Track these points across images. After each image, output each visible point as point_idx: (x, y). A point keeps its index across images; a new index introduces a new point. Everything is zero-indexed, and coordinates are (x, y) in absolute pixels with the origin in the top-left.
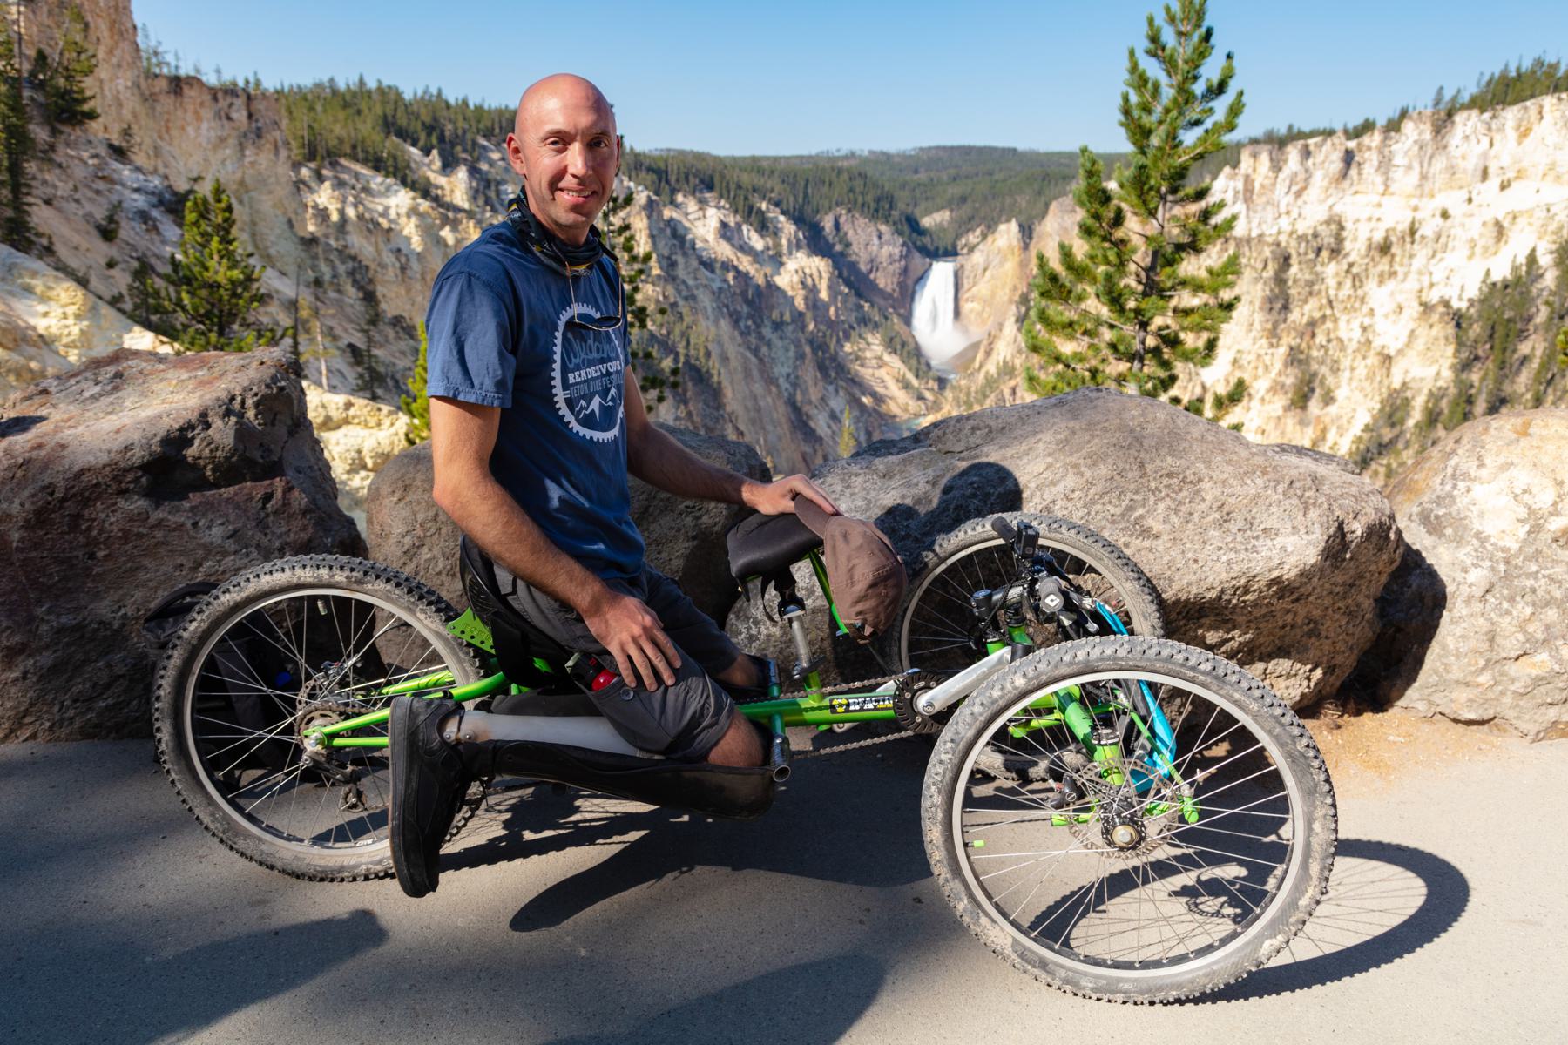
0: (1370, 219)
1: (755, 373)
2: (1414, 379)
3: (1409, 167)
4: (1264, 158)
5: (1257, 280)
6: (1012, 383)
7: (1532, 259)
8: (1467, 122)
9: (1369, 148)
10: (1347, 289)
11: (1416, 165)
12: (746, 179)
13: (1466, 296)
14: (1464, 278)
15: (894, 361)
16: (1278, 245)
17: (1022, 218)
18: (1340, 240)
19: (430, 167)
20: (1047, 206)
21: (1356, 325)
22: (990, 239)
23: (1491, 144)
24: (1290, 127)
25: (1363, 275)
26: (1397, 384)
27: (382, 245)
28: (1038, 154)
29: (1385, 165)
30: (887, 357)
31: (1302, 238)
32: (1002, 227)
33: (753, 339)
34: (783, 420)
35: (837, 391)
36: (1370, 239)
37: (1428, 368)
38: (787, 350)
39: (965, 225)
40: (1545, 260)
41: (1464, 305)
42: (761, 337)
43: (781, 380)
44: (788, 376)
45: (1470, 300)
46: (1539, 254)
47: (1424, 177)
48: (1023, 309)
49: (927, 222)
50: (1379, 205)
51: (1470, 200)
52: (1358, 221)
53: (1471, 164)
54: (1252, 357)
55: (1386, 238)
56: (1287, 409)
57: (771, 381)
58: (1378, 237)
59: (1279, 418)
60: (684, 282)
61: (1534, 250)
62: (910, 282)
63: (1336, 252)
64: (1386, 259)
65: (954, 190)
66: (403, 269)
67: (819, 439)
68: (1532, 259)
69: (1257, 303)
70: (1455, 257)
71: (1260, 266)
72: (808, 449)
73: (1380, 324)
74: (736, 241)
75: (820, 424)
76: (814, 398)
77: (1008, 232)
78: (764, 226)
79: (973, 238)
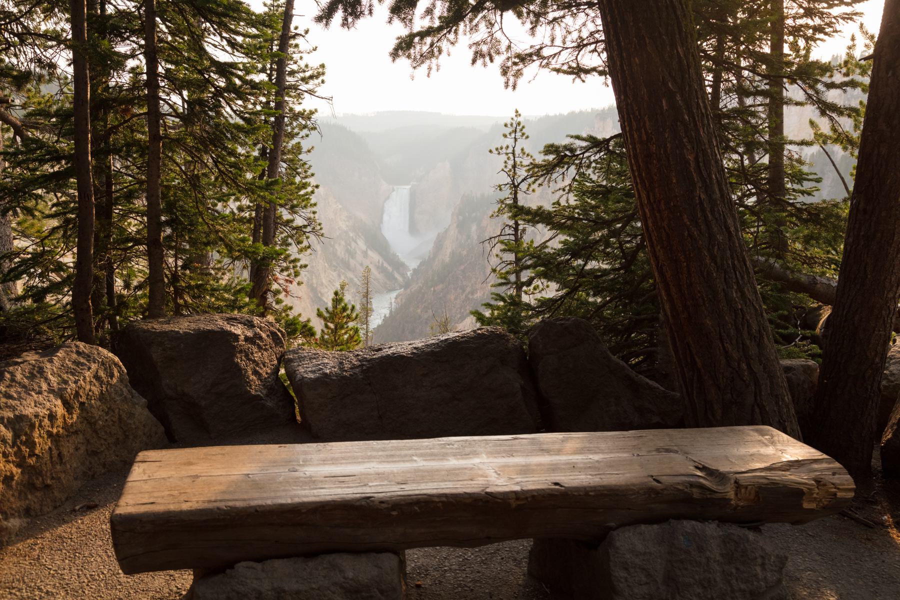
6: (462, 267)
15: (374, 256)
30: (370, 253)
48: (461, 218)
76: (324, 281)
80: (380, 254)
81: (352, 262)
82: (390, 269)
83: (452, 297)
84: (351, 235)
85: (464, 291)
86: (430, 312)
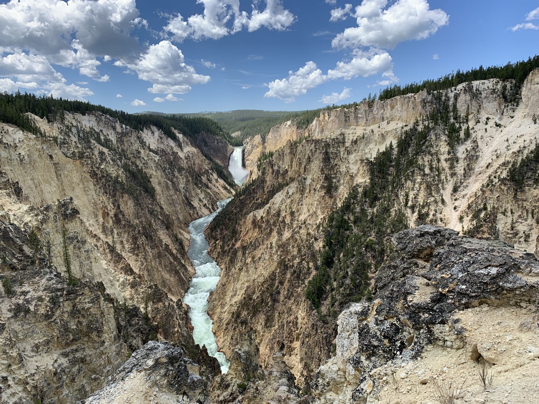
0: (352, 133)
1: (171, 187)
4: (326, 114)
6: (253, 187)
7: (391, 145)
8: (378, 103)
10: (346, 156)
12: (169, 122)
13: (373, 157)
14: (373, 151)
15: (221, 182)
16: (326, 142)
17: (262, 133)
18: (344, 139)
19: (42, 124)
20: (270, 129)
24: (333, 105)
26: (355, 185)
27: (12, 152)
28: (270, 112)
29: (356, 117)
31: (333, 139)
32: (256, 136)
33: (170, 176)
34: (181, 202)
35: (201, 192)
37: (363, 179)
38: (183, 179)
39: (245, 136)
40: (395, 145)
41: (372, 160)
42: (174, 175)
43: (181, 190)
44: (184, 187)
46: (393, 144)
47: (367, 120)
49: (233, 135)
50: (355, 129)
51: (379, 127)
52: (349, 134)
54: (317, 178)
55: (357, 139)
56: (325, 193)
57: (177, 190)
58: (355, 139)
60: (143, 158)
62: (228, 155)
63: (344, 143)
65: (243, 124)
66: (21, 160)
67: (194, 208)
68: (391, 145)
69: (321, 160)
70: (371, 146)
71: (321, 149)
73: (351, 166)
74: (165, 143)
75: (196, 203)
77: (258, 138)
78: (174, 138)
79: (248, 140)
80: (225, 181)
81: (210, 185)
82: (229, 188)
83: (248, 202)
84: (210, 171)
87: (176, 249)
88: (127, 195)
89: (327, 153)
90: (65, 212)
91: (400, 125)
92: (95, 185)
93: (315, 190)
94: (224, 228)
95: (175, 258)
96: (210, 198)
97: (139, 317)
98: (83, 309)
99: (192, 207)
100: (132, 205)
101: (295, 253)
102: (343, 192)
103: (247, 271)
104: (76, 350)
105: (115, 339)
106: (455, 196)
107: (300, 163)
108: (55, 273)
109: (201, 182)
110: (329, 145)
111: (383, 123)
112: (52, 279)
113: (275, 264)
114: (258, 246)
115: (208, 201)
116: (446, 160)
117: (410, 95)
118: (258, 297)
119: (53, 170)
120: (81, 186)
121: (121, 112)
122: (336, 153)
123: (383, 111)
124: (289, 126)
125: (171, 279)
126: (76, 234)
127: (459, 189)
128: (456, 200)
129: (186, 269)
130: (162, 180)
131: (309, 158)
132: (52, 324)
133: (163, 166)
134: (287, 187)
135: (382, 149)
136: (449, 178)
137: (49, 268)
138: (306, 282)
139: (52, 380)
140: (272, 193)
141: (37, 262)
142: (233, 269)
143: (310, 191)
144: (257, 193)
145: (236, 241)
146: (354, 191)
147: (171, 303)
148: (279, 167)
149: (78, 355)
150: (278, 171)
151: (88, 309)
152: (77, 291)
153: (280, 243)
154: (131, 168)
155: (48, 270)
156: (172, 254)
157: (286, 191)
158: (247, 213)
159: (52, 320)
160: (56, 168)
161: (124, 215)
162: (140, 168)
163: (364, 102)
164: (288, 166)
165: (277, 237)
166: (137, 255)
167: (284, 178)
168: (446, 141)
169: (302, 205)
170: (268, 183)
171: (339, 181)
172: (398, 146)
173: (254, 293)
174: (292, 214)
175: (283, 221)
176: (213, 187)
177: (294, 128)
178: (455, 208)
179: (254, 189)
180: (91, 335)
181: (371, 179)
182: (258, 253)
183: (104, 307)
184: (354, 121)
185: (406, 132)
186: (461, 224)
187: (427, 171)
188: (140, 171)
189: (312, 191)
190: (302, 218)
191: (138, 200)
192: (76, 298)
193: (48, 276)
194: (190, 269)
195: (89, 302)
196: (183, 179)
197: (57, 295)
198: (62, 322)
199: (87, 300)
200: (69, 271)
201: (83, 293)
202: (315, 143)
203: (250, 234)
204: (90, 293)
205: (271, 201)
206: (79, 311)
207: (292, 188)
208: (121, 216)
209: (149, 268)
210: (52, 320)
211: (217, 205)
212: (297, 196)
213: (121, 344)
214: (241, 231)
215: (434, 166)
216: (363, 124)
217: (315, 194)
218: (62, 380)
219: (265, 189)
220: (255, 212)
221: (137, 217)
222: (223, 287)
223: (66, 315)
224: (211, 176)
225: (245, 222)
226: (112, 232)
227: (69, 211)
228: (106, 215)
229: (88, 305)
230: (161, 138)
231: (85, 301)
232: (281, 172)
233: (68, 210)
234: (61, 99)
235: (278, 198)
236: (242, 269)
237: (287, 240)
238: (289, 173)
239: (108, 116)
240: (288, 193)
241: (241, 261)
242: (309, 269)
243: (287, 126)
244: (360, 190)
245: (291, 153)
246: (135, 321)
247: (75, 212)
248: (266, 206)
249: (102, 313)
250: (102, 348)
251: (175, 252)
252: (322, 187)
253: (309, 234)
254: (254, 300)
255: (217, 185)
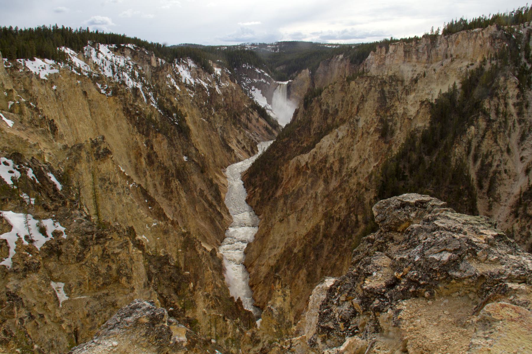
2: (418, 127)
3: (424, 53)
4: (384, 49)
5: (376, 91)
6: (298, 129)
9: (411, 46)
11: (426, 53)
15: (262, 121)
16: (383, 79)
20: (319, 63)
21: (402, 108)
22: (299, 76)
23: (448, 47)
24: (392, 38)
25: (409, 90)
26: (413, 129)
28: (320, 44)
31: (391, 77)
32: (304, 71)
33: (207, 114)
35: (240, 132)
36: (412, 77)
37: (422, 123)
38: (220, 118)
40: (459, 86)
43: (218, 129)
44: (221, 127)
45: (436, 100)
53: (441, 53)
55: (417, 77)
56: (379, 138)
58: (415, 77)
59: (378, 141)
61: (455, 83)
64: (416, 85)
69: (376, 99)
70: (433, 86)
71: (377, 87)
72: (228, 155)
73: (409, 107)
75: (233, 145)
77: (306, 73)
79: (294, 75)
80: (266, 120)
81: (249, 125)
83: (292, 145)
85: (299, 142)
86: (280, 154)
87: (211, 195)
88: (160, 135)
89: (382, 92)
90: (97, 152)
91: (466, 63)
92: (128, 124)
93: (368, 133)
94: (264, 173)
95: (211, 205)
96: (249, 139)
97: (171, 265)
98: (113, 253)
99: (230, 150)
100: (166, 146)
101: (343, 205)
102: (400, 137)
103: (288, 222)
104: (107, 295)
105: (145, 287)
106: (522, 145)
107: (352, 103)
108: (85, 215)
109: (240, 121)
110: (385, 82)
111: (446, 60)
112: (82, 221)
113: (320, 215)
114: (302, 196)
115: (247, 143)
116: (514, 105)
117: (477, 30)
118: (299, 251)
119: (87, 108)
120: (114, 125)
121: (158, 44)
122: (393, 93)
123: (446, 46)
124: (342, 60)
125: (205, 225)
126: (108, 176)
127: (527, 138)
128: (523, 150)
129: (222, 217)
130: (197, 118)
131: (363, 96)
132: (84, 266)
133: (199, 104)
134: (336, 130)
135: (445, 90)
136: (517, 125)
137: (79, 210)
138: (354, 236)
139: (85, 321)
140: (320, 136)
141: (68, 203)
142: (273, 220)
143: (363, 134)
144: (301, 135)
145: (277, 188)
146: (411, 137)
147: (205, 252)
148: (328, 106)
149: (109, 299)
150: (327, 112)
151: (118, 254)
152: (106, 235)
153: (327, 193)
154: (165, 106)
155: (78, 212)
156: (207, 201)
157: (335, 134)
158: (291, 158)
159: (83, 263)
160: (90, 105)
161: (157, 156)
162: (175, 105)
163: (426, 36)
164: (339, 105)
165: (323, 186)
166: (171, 200)
167: (333, 120)
168: (515, 82)
169: (353, 150)
170: (315, 125)
171: (395, 124)
172: (462, 88)
173: (295, 246)
174: (341, 161)
175: (331, 168)
176: (253, 127)
177: (347, 62)
178: (522, 159)
179: (299, 131)
180: (120, 280)
181: (431, 123)
182: (300, 204)
183: (133, 253)
184: (414, 57)
185: (472, 72)
186: (527, 177)
187: (493, 116)
188: (175, 109)
189: (365, 136)
190: (352, 165)
191: (172, 140)
192: (105, 243)
193: (78, 218)
194: (226, 217)
195: (118, 248)
196: (220, 118)
197: (87, 238)
198: (93, 266)
199: (117, 245)
200: (97, 214)
201: (112, 238)
202: (370, 80)
203: (293, 181)
204: (119, 238)
205: (318, 145)
206: (108, 255)
207: (342, 131)
208: (153, 158)
209: (183, 213)
210: (83, 263)
211: (257, 148)
212: (348, 140)
213: (151, 292)
214: (283, 178)
215: (501, 111)
216: (424, 61)
217: (367, 138)
218: (95, 322)
219: (312, 131)
220: (299, 157)
221: (171, 158)
222: (261, 238)
223: (96, 258)
224: (251, 115)
225: (287, 168)
226: (145, 173)
227: (102, 151)
228: (139, 155)
229: (117, 251)
230: (198, 72)
231: (113, 245)
232: (330, 112)
233: (100, 150)
234: (97, 32)
235: (326, 141)
236: (283, 220)
237: (334, 190)
238: (339, 112)
239: (144, 49)
240: (337, 136)
241: (282, 211)
242: (357, 222)
243: (339, 60)
244: (419, 135)
245: (342, 90)
246: (166, 268)
247: (107, 152)
248: (312, 151)
249: (131, 259)
250: (132, 295)
251: (210, 198)
252: (376, 130)
253: (359, 184)
254: (295, 254)
255: (257, 125)
